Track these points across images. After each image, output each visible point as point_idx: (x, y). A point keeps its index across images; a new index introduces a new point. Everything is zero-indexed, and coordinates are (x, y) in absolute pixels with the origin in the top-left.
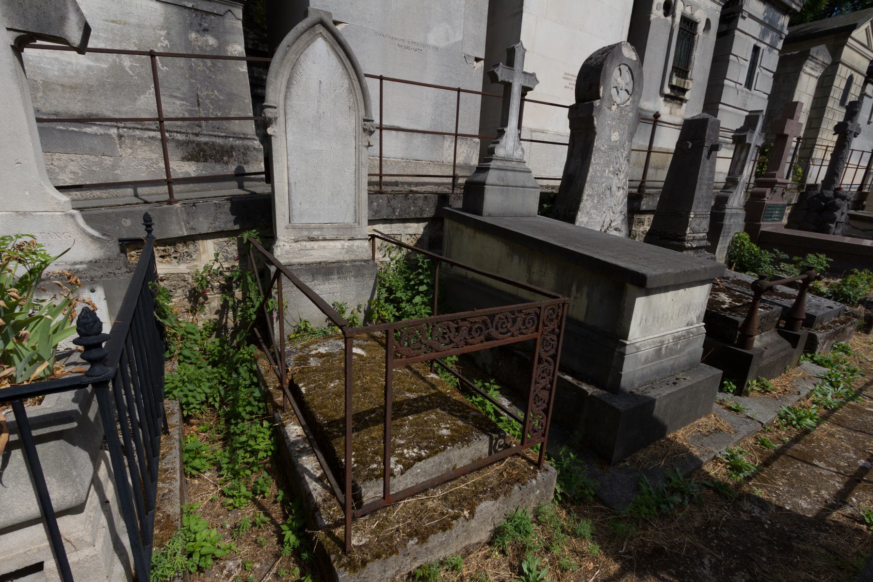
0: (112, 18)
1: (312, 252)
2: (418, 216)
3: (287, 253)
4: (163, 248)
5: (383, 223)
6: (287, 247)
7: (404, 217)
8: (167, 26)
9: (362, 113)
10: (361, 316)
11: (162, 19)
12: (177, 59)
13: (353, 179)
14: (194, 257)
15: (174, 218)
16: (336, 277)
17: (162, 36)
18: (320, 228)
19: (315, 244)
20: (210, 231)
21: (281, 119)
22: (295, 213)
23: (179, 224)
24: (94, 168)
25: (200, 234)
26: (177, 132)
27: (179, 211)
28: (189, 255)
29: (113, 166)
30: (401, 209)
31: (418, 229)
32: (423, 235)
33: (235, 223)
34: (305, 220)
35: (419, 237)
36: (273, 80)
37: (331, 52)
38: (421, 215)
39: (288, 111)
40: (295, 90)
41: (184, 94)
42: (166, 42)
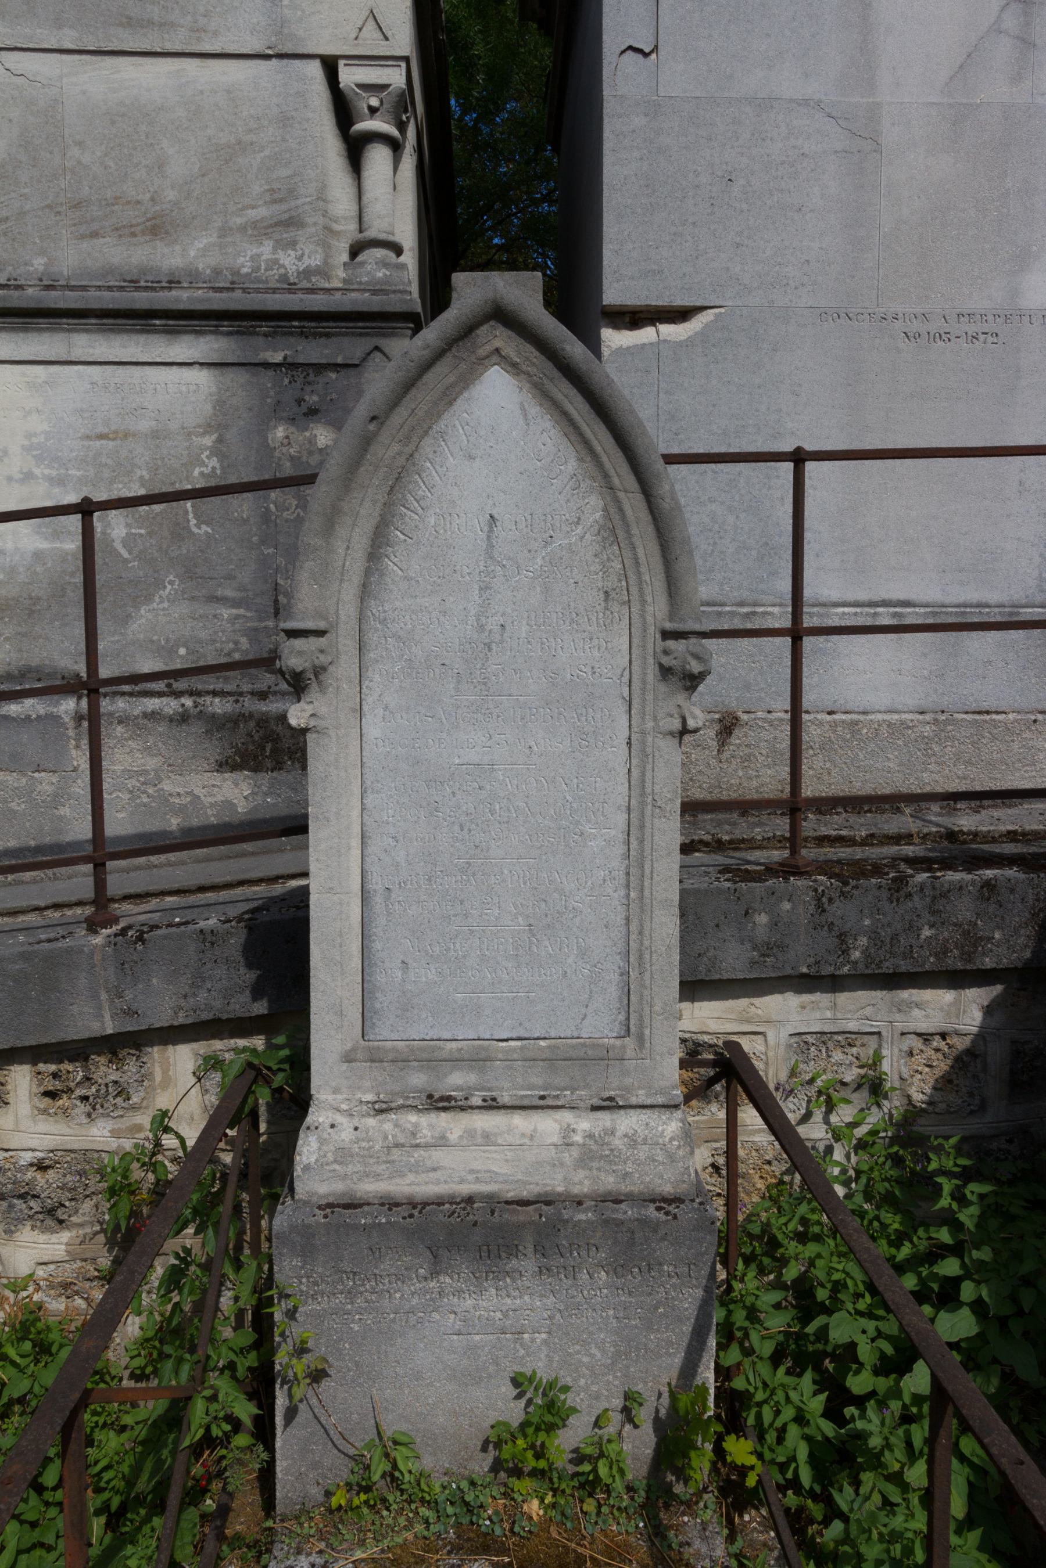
0: (101, 429)
1: (438, 1156)
2: (954, 961)
3: (343, 1155)
4: (53, 1068)
5: (799, 991)
6: (346, 1134)
7: (887, 967)
8: (218, 425)
9: (657, 609)
10: (638, 1446)
11: (208, 408)
12: (234, 500)
13: (617, 864)
14: (135, 1099)
15: (83, 982)
16: (528, 1264)
17: (203, 449)
18: (478, 1059)
19: (452, 1125)
20: (181, 1020)
21: (344, 669)
22: (382, 1001)
23: (95, 997)
24: (13, 805)
25: (150, 1031)
26: (215, 693)
27: (97, 957)
28: (123, 1092)
29: (56, 795)
30: (874, 935)
31: (958, 1012)
32: (981, 1036)
33: (257, 993)
34: (421, 1029)
35: (961, 1044)
36: (317, 541)
37: (535, 410)
38: (968, 957)
39: (373, 638)
40: (402, 563)
41: (242, 588)
42: (214, 462)
